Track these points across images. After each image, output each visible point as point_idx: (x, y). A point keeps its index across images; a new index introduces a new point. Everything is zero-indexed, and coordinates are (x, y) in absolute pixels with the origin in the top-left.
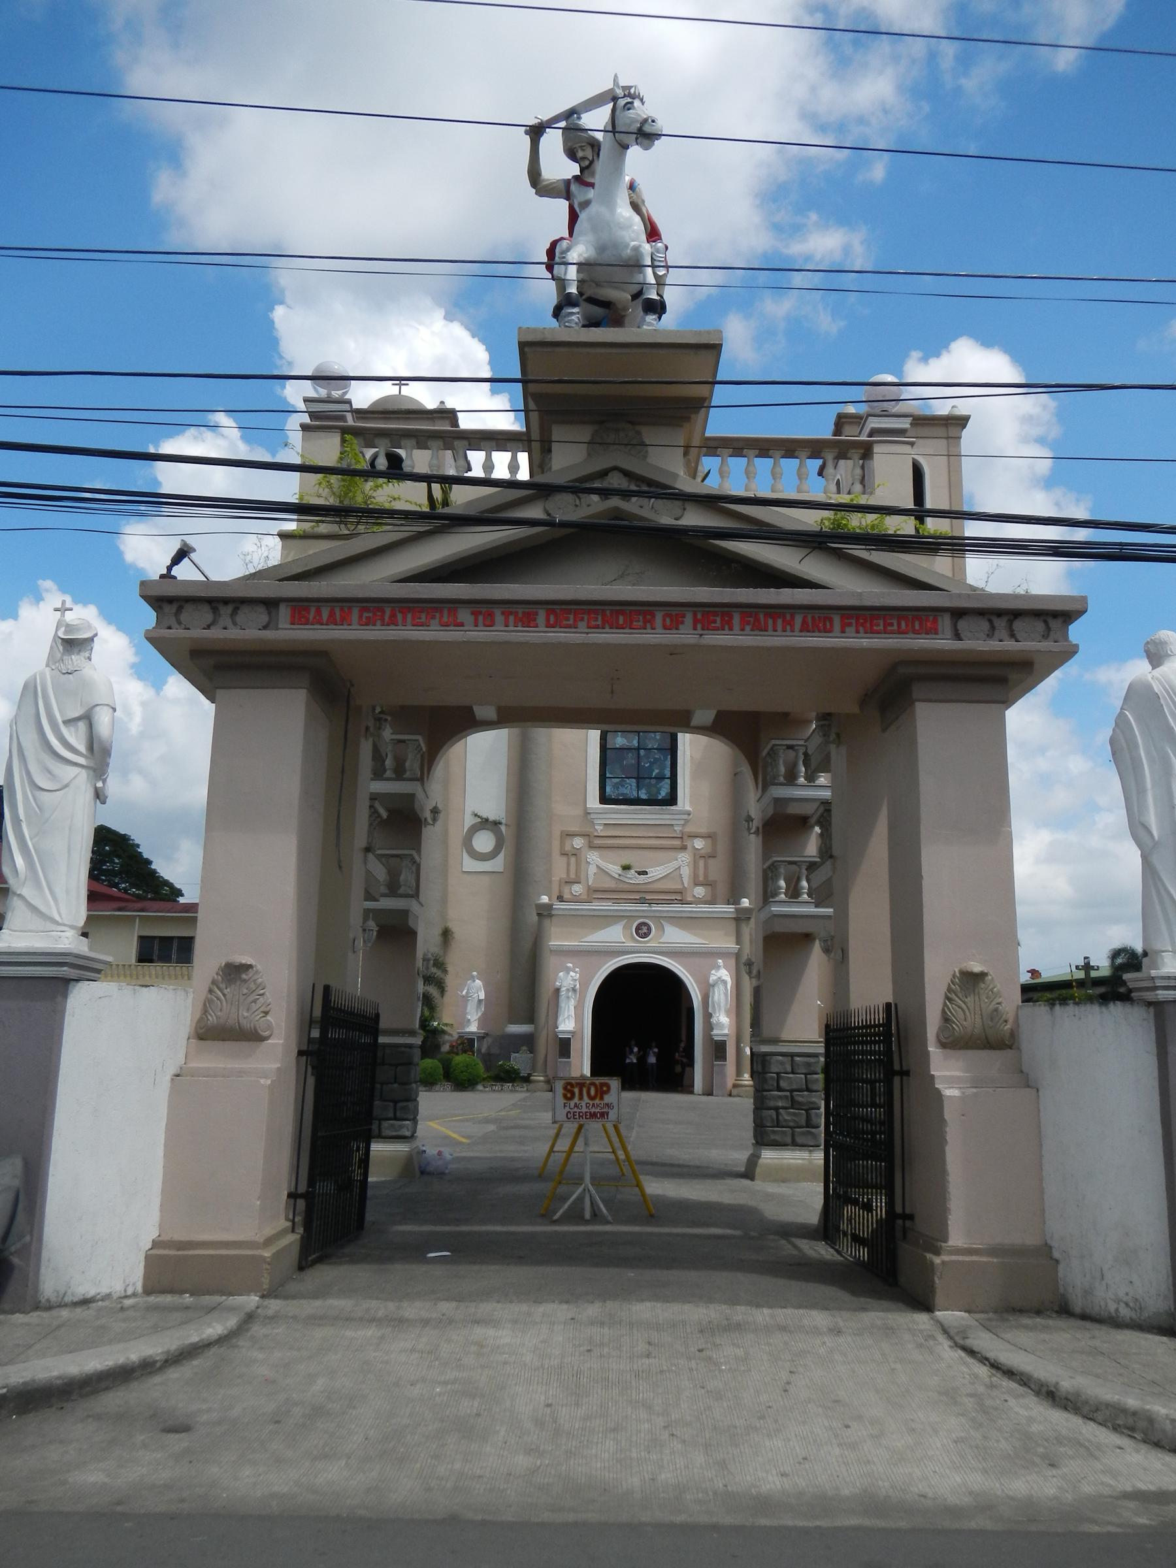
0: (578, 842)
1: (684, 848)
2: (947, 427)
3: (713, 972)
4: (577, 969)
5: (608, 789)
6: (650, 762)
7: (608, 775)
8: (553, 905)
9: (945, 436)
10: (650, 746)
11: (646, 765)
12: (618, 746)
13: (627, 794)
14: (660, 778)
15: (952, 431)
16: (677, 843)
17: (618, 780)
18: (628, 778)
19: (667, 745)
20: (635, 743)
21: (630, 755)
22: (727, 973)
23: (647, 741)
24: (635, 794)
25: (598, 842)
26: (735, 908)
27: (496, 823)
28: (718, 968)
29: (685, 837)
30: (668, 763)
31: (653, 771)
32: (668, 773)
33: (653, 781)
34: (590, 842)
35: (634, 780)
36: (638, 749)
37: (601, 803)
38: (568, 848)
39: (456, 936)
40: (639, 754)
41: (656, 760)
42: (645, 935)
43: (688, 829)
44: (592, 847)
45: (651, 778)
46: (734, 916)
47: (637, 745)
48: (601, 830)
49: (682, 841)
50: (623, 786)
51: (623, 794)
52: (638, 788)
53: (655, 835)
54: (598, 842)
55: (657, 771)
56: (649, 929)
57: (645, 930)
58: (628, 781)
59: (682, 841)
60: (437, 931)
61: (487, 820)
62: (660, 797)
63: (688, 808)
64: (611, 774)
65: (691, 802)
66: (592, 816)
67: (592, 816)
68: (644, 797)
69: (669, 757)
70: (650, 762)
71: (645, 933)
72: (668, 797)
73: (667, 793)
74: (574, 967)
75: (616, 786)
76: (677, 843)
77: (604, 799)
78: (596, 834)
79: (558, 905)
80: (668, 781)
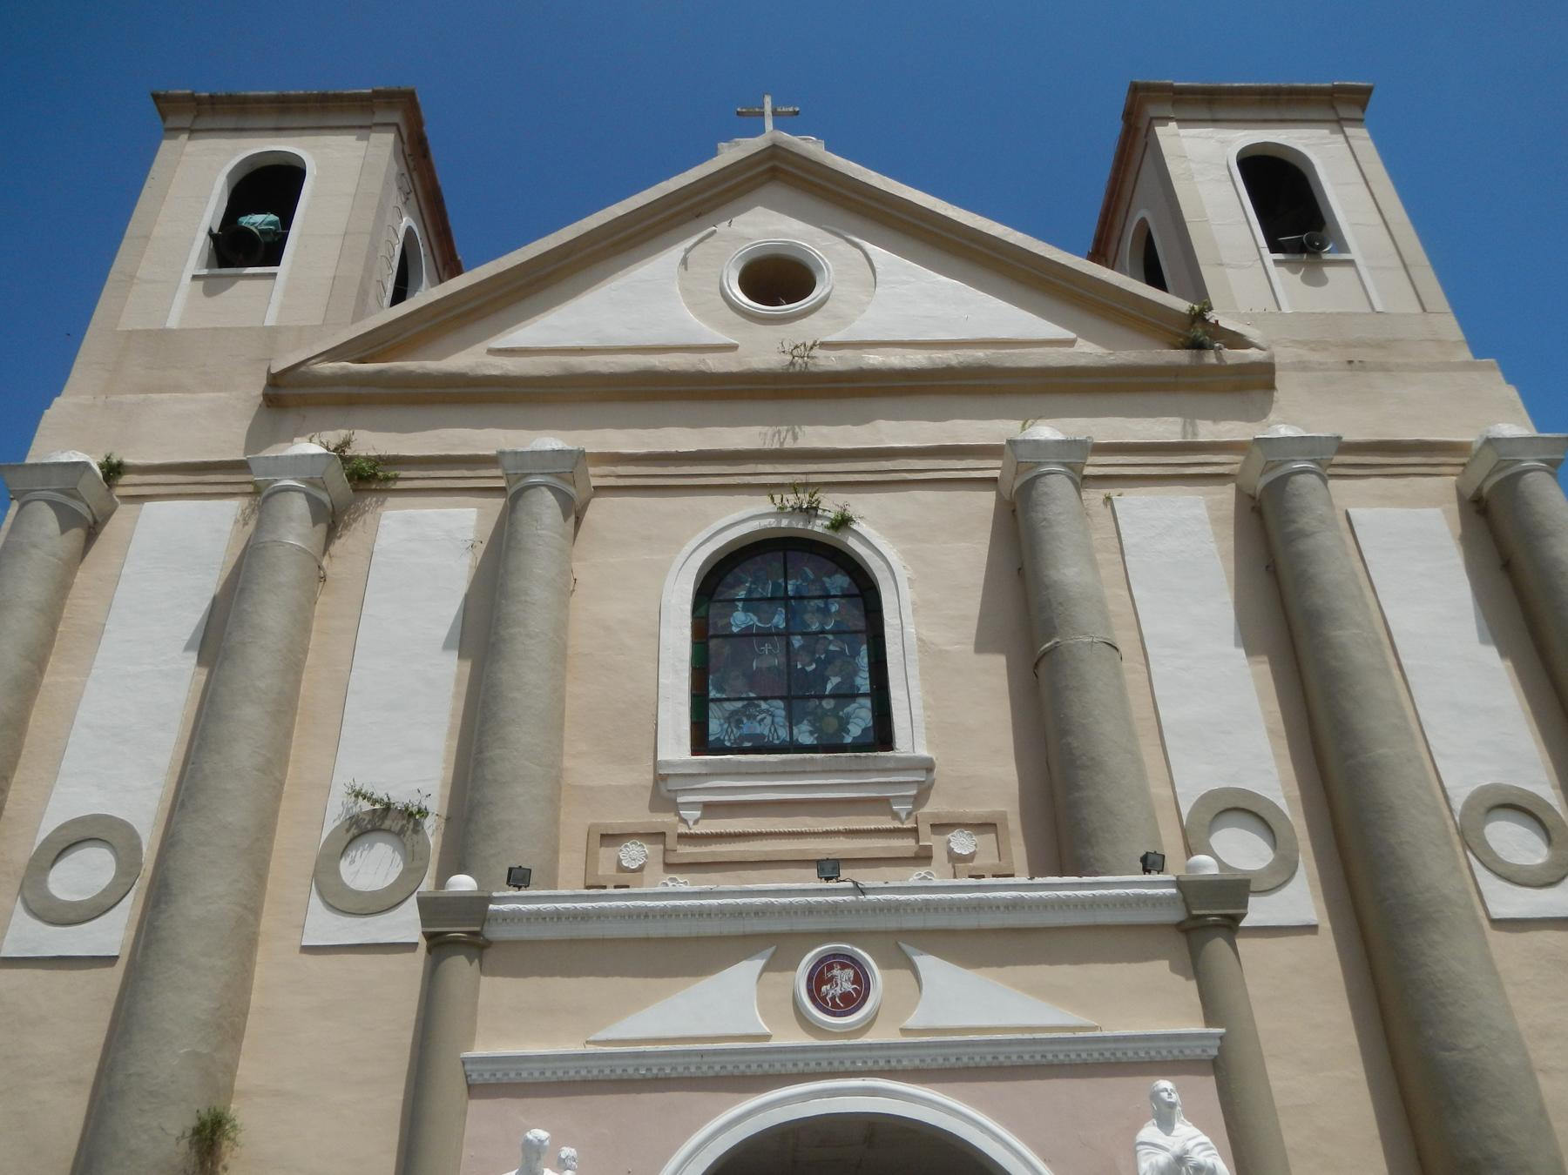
0: (632, 854)
1: (923, 857)
2: (1333, 107)
3: (1150, 1132)
4: (567, 1152)
5: (715, 727)
6: (818, 661)
7: (713, 694)
8: (491, 900)
9: (1335, 118)
10: (815, 627)
11: (809, 669)
12: (735, 630)
13: (762, 736)
14: (847, 695)
15: (1344, 112)
16: (906, 845)
17: (739, 704)
18: (765, 699)
19: (861, 624)
20: (779, 620)
21: (767, 647)
22: (1205, 1139)
23: (807, 617)
24: (783, 733)
25: (687, 851)
26: (1178, 884)
27: (413, 817)
28: (1166, 1124)
29: (924, 829)
30: (863, 660)
31: (825, 680)
32: (863, 682)
33: (828, 704)
34: (665, 851)
35: (781, 704)
36: (786, 634)
37: (692, 755)
38: (606, 868)
39: (241, 1138)
40: (789, 644)
41: (831, 657)
42: (850, 1003)
43: (935, 806)
44: (669, 867)
45: (822, 697)
46: (1176, 915)
47: (782, 625)
48: (696, 822)
49: (918, 842)
50: (751, 717)
51: (749, 737)
52: (792, 720)
53: (841, 828)
54: (687, 851)
55: (833, 682)
56: (862, 981)
57: (844, 981)
58: (764, 705)
59: (918, 842)
60: (178, 1122)
61: (388, 807)
62: (848, 740)
63: (922, 752)
64: (720, 689)
65: (930, 743)
66: (673, 784)
67: (673, 784)
68: (806, 739)
69: (864, 647)
70: (818, 661)
71: (846, 997)
72: (870, 738)
73: (865, 730)
74: (560, 1138)
75: (734, 719)
76: (906, 845)
77: (701, 742)
78: (683, 829)
79: (508, 901)
80: (867, 702)
